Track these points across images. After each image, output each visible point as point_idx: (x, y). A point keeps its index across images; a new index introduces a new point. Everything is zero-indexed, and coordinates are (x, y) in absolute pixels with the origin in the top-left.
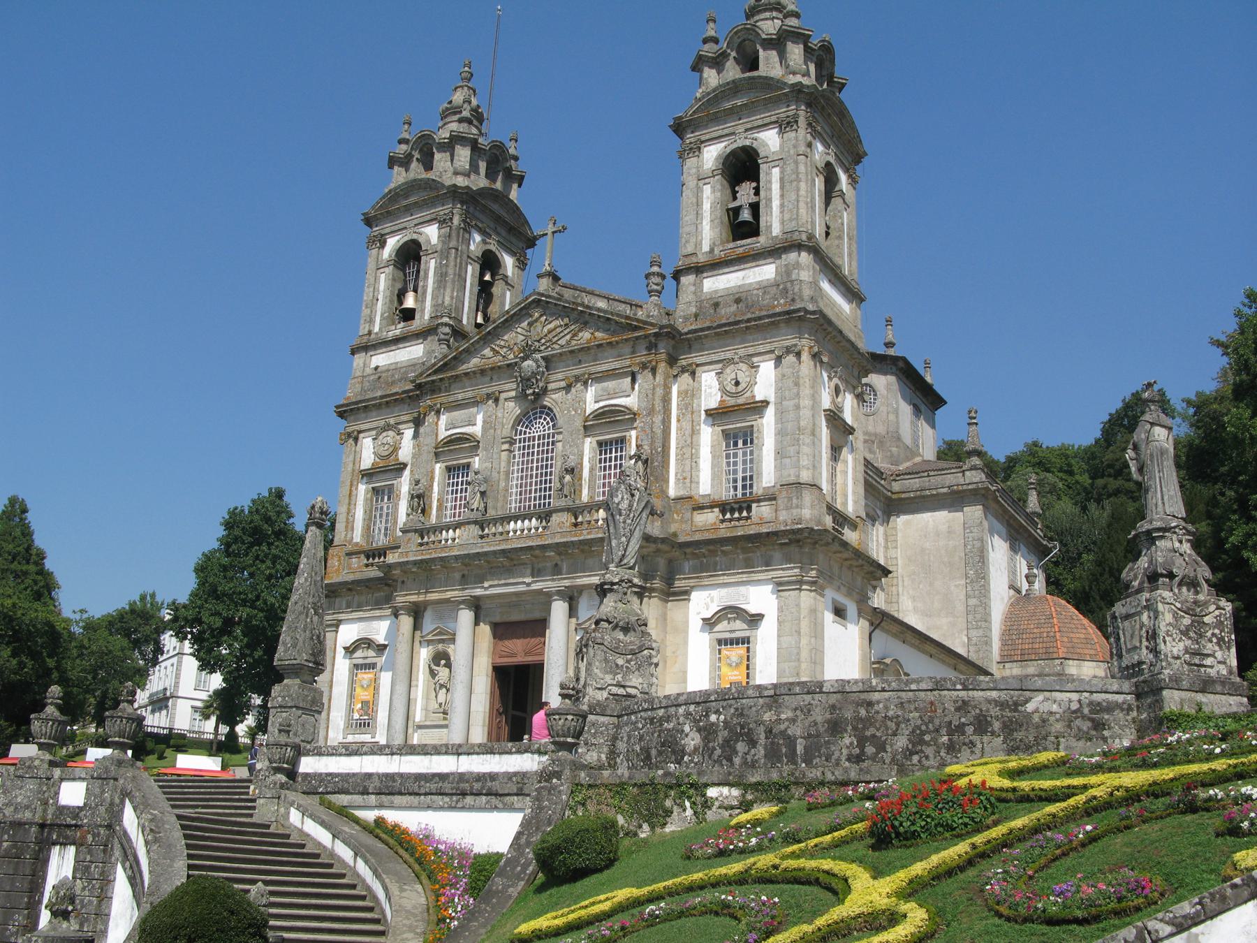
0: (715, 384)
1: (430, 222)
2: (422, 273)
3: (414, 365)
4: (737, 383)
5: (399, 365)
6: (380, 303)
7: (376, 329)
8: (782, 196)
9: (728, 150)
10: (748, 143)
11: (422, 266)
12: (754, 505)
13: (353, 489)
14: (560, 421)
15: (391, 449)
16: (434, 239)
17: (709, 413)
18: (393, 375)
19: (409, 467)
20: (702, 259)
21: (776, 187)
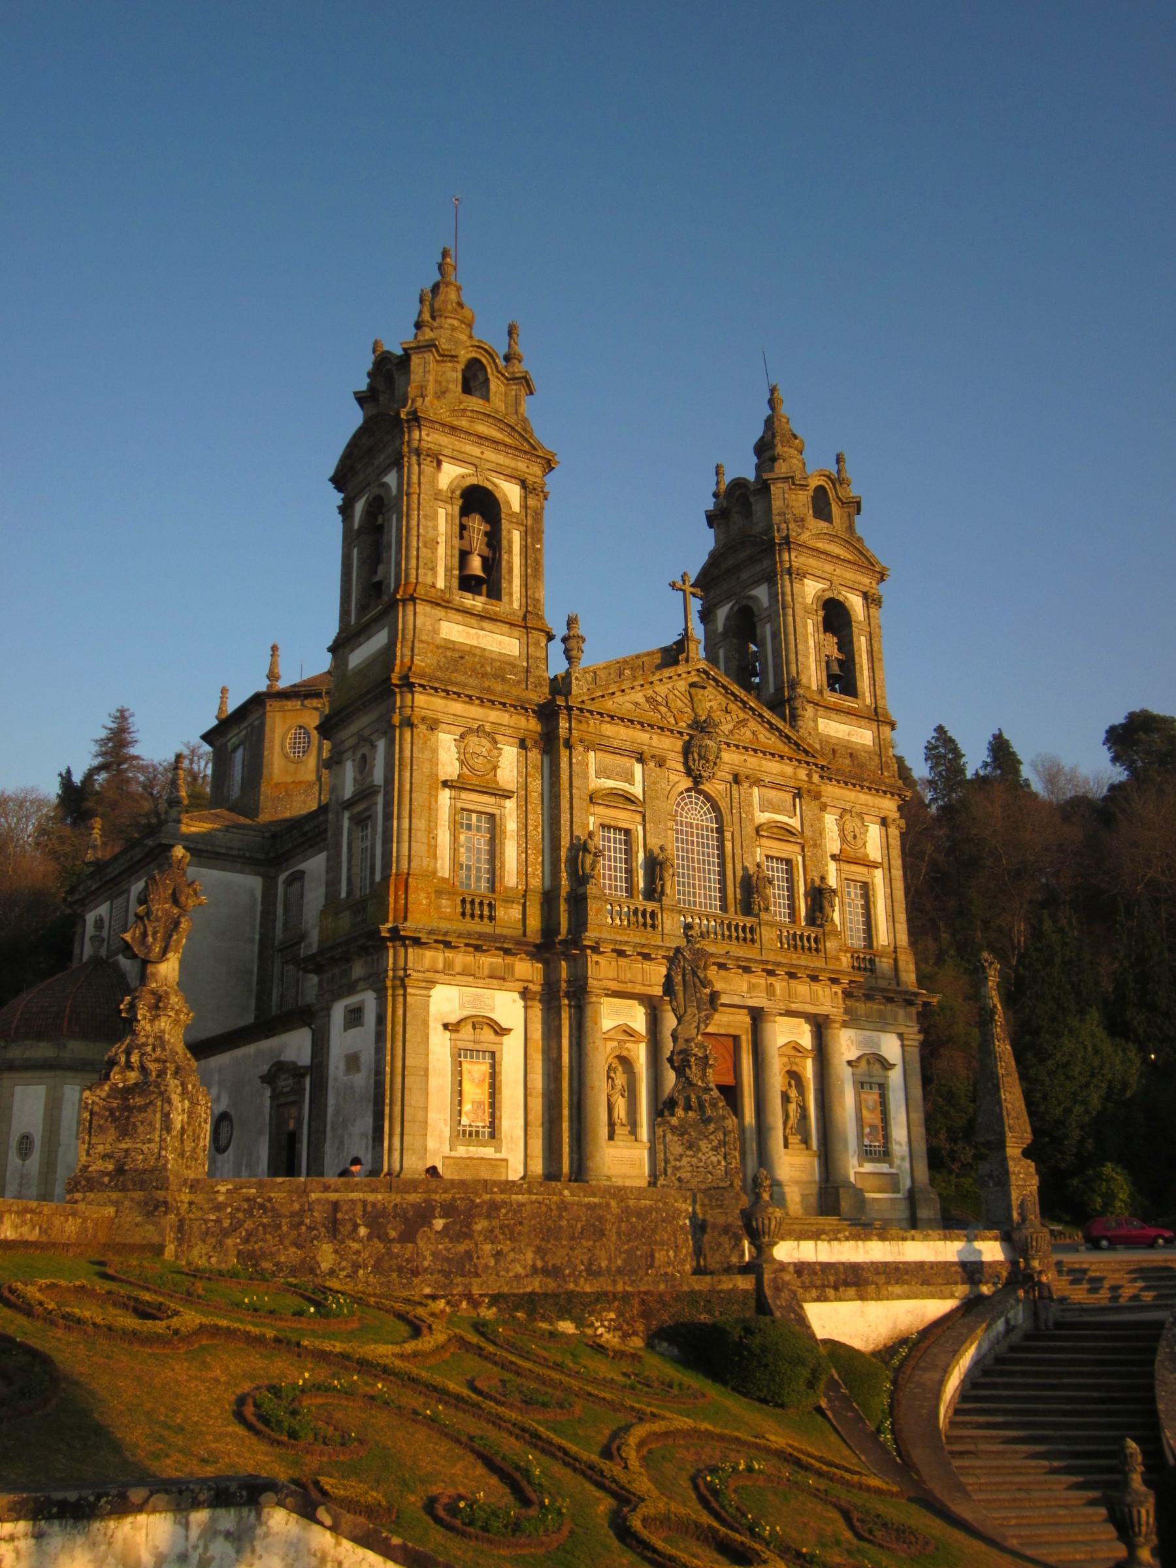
0: (835, 828)
1: (511, 477)
2: (504, 543)
3: (514, 666)
4: (855, 837)
5: (487, 654)
6: (441, 550)
7: (441, 584)
8: (872, 669)
9: (828, 595)
10: (841, 599)
11: (504, 533)
12: (877, 959)
13: (433, 799)
14: (727, 818)
15: (489, 766)
16: (516, 506)
17: (834, 857)
18: (482, 666)
19: (514, 799)
20: (816, 698)
21: (864, 656)
